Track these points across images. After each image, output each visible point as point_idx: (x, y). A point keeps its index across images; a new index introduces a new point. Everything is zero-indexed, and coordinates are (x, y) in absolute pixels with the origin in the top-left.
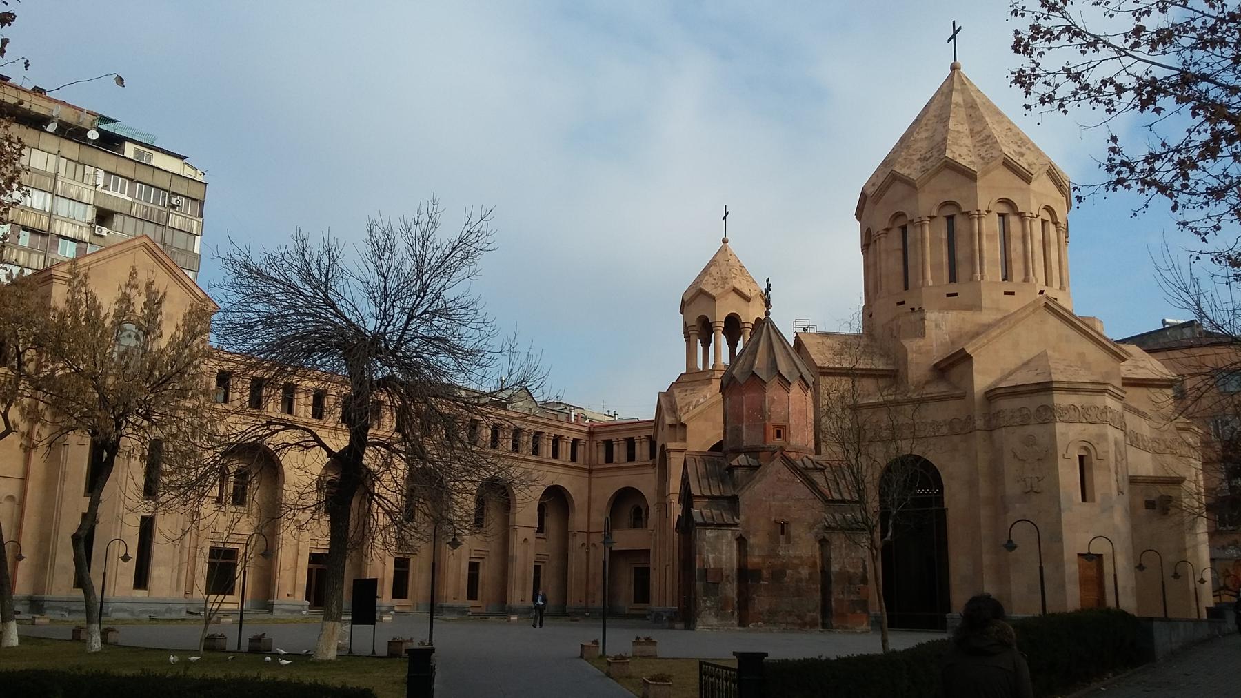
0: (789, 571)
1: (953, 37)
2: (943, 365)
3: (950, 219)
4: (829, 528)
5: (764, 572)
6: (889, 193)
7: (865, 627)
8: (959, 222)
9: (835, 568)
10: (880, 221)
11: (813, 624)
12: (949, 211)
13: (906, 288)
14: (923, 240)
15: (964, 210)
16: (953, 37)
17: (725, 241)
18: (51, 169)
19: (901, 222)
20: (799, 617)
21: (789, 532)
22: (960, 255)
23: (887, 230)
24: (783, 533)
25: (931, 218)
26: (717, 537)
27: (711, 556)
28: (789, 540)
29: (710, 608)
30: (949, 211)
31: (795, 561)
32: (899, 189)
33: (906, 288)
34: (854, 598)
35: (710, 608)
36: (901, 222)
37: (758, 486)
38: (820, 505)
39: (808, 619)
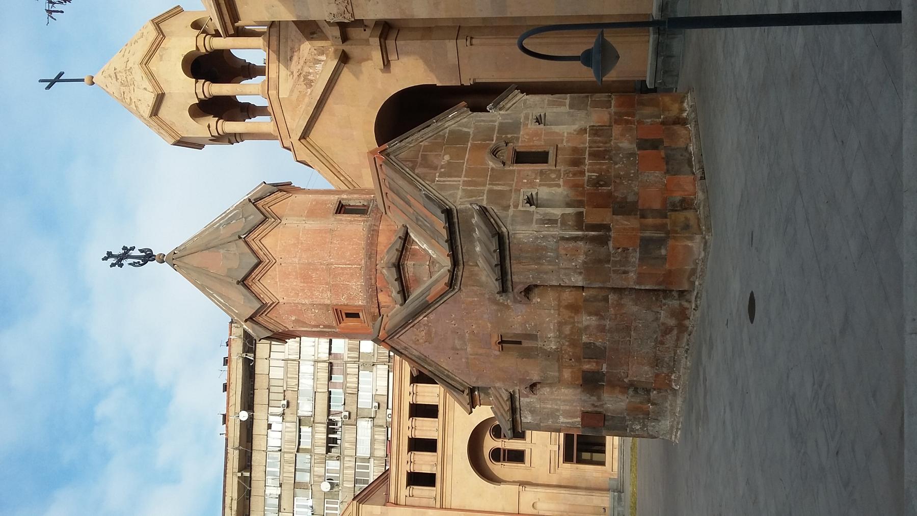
0: (585, 339)
4: (504, 290)
5: (586, 367)
7: (695, 244)
9: (578, 280)
11: (681, 315)
18: (282, 363)
20: (667, 331)
21: (516, 335)
24: (520, 343)
26: (533, 412)
27: (562, 419)
28: (531, 337)
29: (644, 426)
31: (567, 330)
34: (635, 257)
35: (644, 426)
37: (444, 365)
38: (465, 295)
39: (672, 322)
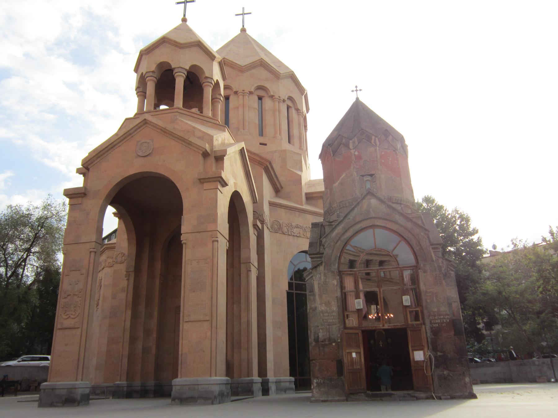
1: (243, 14)
2: (314, 195)
3: (288, 107)
6: (253, 71)
8: (293, 112)
10: (245, 83)
12: (290, 104)
13: (261, 134)
14: (279, 112)
15: (299, 107)
16: (243, 14)
17: (184, 20)
19: (261, 93)
22: (295, 132)
23: (251, 93)
25: (284, 101)
30: (290, 104)
32: (264, 73)
33: (261, 134)
36: (261, 93)
